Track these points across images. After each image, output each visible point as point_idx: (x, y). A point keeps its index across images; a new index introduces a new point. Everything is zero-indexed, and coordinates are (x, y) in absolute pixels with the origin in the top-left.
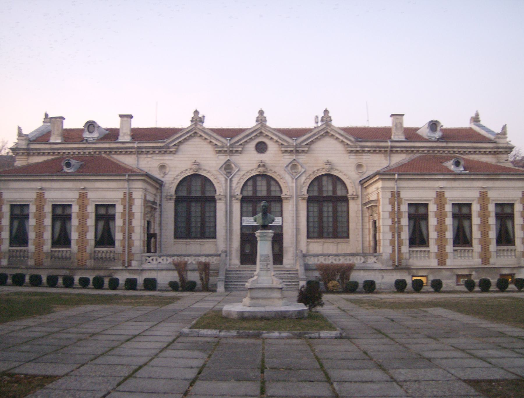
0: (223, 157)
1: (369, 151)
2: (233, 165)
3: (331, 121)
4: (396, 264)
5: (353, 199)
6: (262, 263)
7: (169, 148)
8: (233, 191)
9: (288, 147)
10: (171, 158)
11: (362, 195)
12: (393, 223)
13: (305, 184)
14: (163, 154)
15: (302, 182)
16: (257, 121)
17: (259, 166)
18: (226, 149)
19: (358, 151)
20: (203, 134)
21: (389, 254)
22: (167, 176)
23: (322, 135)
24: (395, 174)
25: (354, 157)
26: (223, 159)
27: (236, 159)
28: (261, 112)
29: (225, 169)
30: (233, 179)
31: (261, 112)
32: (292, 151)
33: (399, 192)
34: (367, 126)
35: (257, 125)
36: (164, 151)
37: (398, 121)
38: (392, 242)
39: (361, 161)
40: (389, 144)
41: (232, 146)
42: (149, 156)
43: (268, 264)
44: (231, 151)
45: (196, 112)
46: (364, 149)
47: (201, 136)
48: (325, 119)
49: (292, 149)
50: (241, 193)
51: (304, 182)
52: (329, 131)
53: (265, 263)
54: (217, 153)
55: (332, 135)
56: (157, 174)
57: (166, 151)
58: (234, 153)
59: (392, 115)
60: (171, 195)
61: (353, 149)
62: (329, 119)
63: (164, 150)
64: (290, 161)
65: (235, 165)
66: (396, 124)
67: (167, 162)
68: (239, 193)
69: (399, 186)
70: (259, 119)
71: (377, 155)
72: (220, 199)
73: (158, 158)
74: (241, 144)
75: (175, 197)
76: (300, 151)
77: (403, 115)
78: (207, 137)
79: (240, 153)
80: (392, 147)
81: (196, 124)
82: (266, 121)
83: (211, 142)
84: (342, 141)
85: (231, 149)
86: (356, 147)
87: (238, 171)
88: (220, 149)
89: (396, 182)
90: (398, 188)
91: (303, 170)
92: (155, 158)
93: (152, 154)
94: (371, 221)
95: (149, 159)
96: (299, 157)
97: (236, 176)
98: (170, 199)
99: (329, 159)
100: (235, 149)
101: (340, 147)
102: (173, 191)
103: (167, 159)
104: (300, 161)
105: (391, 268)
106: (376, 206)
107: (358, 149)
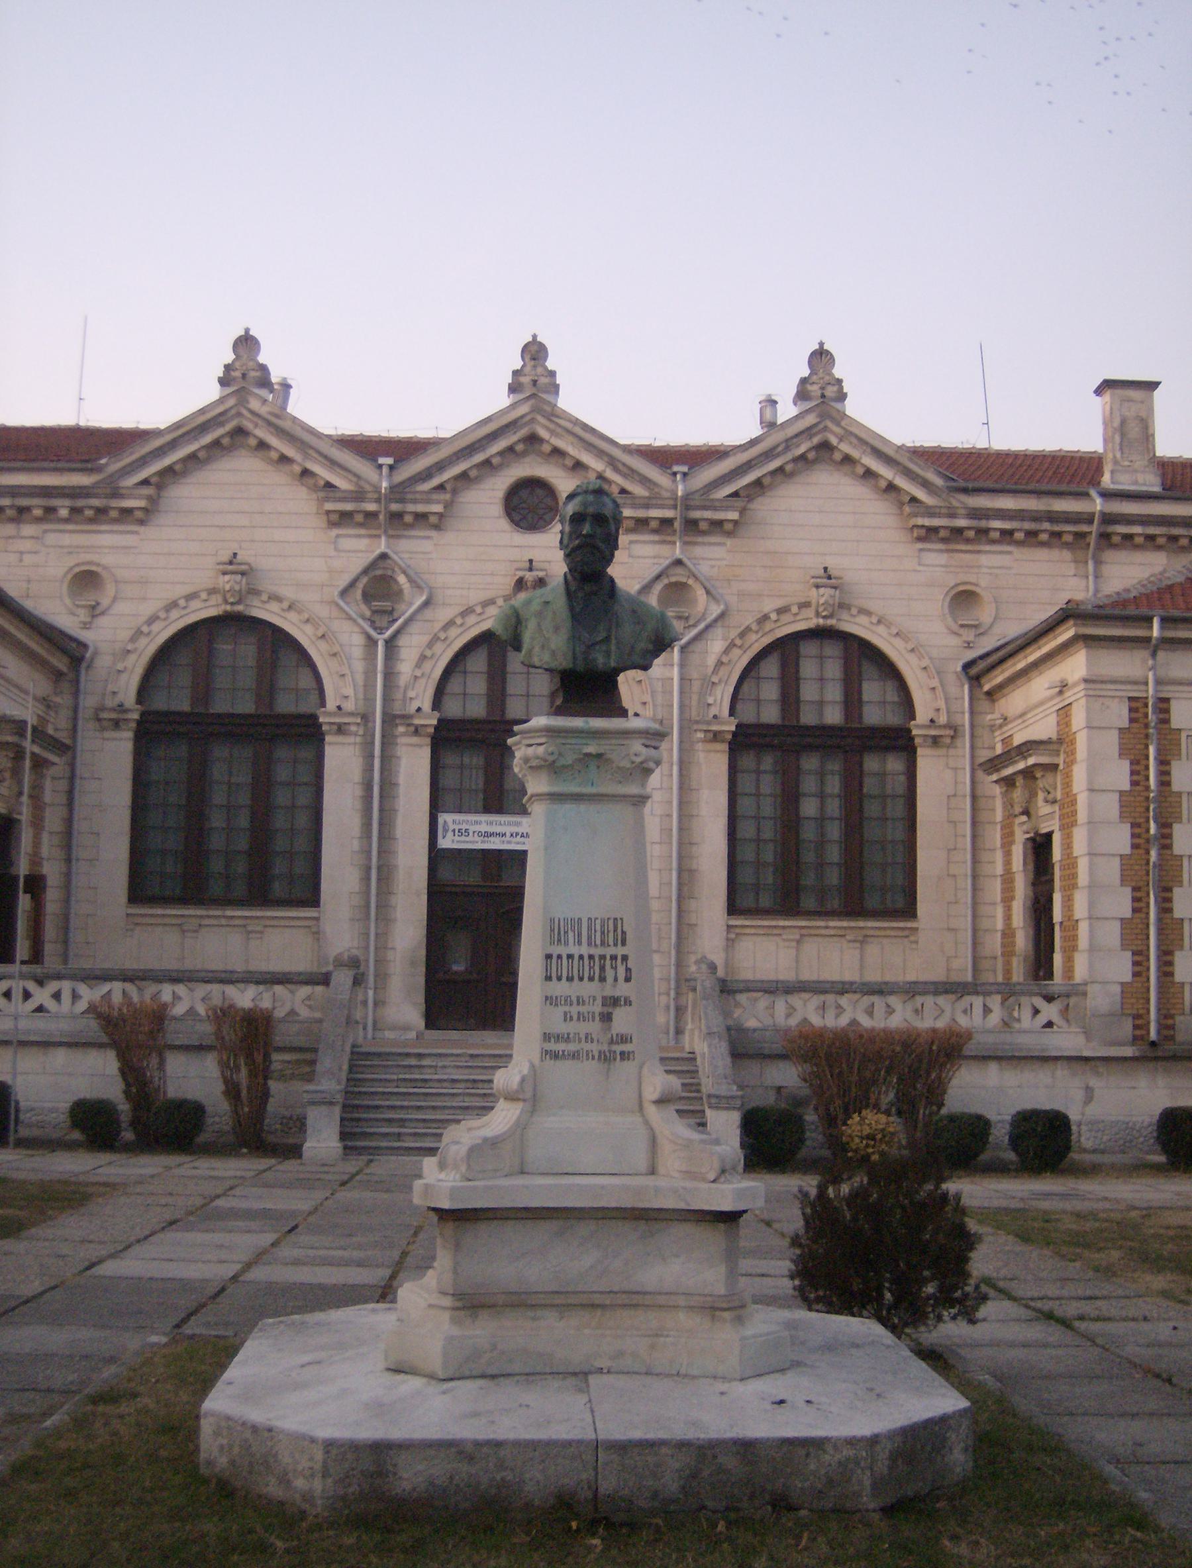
0: (363, 543)
1: (1007, 535)
2: (402, 579)
3: (842, 397)
4: (1153, 1035)
5: (935, 741)
6: (560, 988)
7: (116, 494)
8: (399, 695)
9: (647, 506)
10: (128, 540)
11: (972, 726)
12: (1140, 841)
13: (723, 671)
14: (91, 521)
15: (711, 661)
16: (513, 389)
17: (520, 584)
18: (371, 507)
19: (958, 531)
20: (273, 441)
21: (1118, 989)
22: (103, 621)
23: (803, 457)
24: (1149, 620)
25: (943, 559)
26: (357, 550)
27: (416, 551)
28: (535, 351)
29: (367, 597)
30: (402, 641)
31: (535, 351)
32: (666, 523)
33: (1167, 700)
34: (981, 444)
35: (513, 406)
36: (98, 510)
37: (1131, 411)
38: (1133, 934)
39: (972, 579)
40: (1098, 505)
41: (399, 492)
42: (28, 530)
43: (615, 1002)
44: (396, 517)
45: (246, 343)
46: (983, 524)
47: (262, 445)
48: (814, 389)
49: (669, 514)
50: (437, 704)
51: (720, 664)
52: (834, 441)
53: (589, 989)
54: (333, 524)
55: (847, 460)
56: (61, 613)
57: (101, 511)
58: (410, 526)
59: (1108, 385)
60: (121, 709)
61: (936, 522)
62: (831, 391)
63: (96, 502)
64: (657, 570)
65: (411, 580)
66: (1123, 422)
67: (108, 559)
68: (427, 706)
69: (1162, 673)
70: (525, 380)
71: (1042, 554)
72: (341, 729)
73: (67, 539)
74: (441, 487)
75: (136, 716)
76: (703, 526)
77: (1152, 386)
78: (290, 452)
79: (437, 527)
80: (1109, 519)
81: (242, 395)
82: (555, 389)
83: (305, 472)
84: (891, 487)
85: (395, 507)
86: (952, 516)
87: (426, 604)
88: (348, 507)
89: (1154, 655)
90: (1158, 682)
91: (715, 610)
92: (51, 538)
93: (39, 520)
94: (1020, 837)
95: (28, 545)
96: (698, 551)
97: (415, 627)
98: (116, 724)
99: (831, 562)
100: (411, 508)
101: (878, 513)
102: (127, 687)
103: (107, 546)
104: (704, 569)
105: (1128, 1051)
106: (1054, 767)
107: (962, 523)
